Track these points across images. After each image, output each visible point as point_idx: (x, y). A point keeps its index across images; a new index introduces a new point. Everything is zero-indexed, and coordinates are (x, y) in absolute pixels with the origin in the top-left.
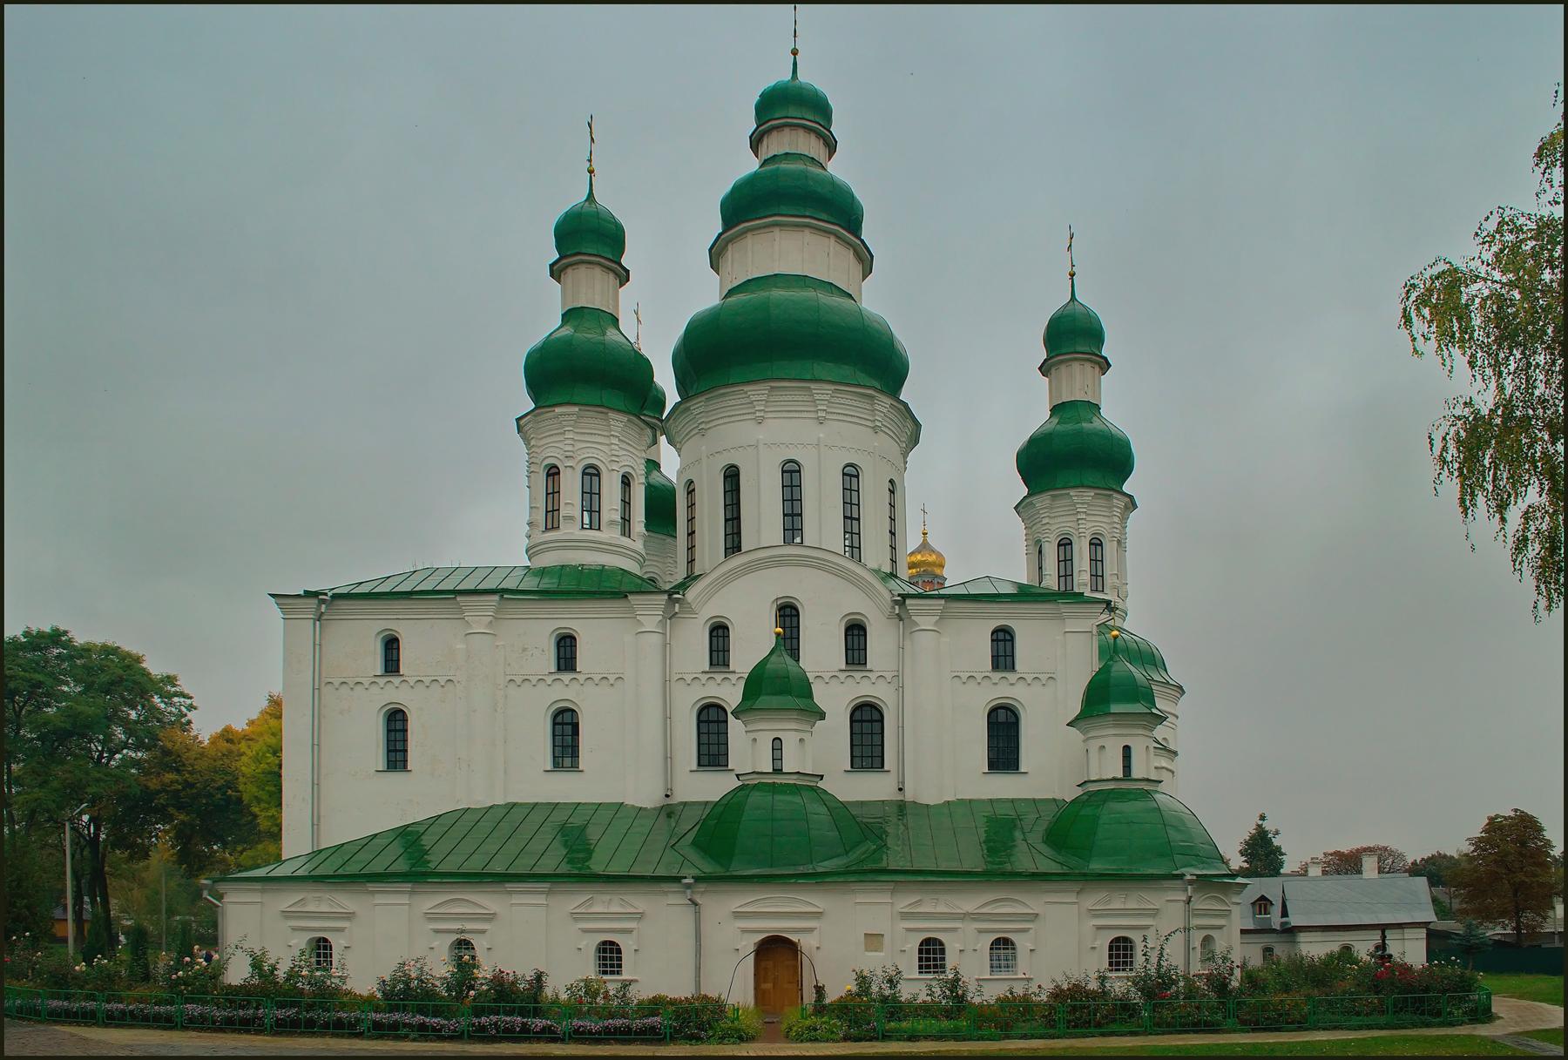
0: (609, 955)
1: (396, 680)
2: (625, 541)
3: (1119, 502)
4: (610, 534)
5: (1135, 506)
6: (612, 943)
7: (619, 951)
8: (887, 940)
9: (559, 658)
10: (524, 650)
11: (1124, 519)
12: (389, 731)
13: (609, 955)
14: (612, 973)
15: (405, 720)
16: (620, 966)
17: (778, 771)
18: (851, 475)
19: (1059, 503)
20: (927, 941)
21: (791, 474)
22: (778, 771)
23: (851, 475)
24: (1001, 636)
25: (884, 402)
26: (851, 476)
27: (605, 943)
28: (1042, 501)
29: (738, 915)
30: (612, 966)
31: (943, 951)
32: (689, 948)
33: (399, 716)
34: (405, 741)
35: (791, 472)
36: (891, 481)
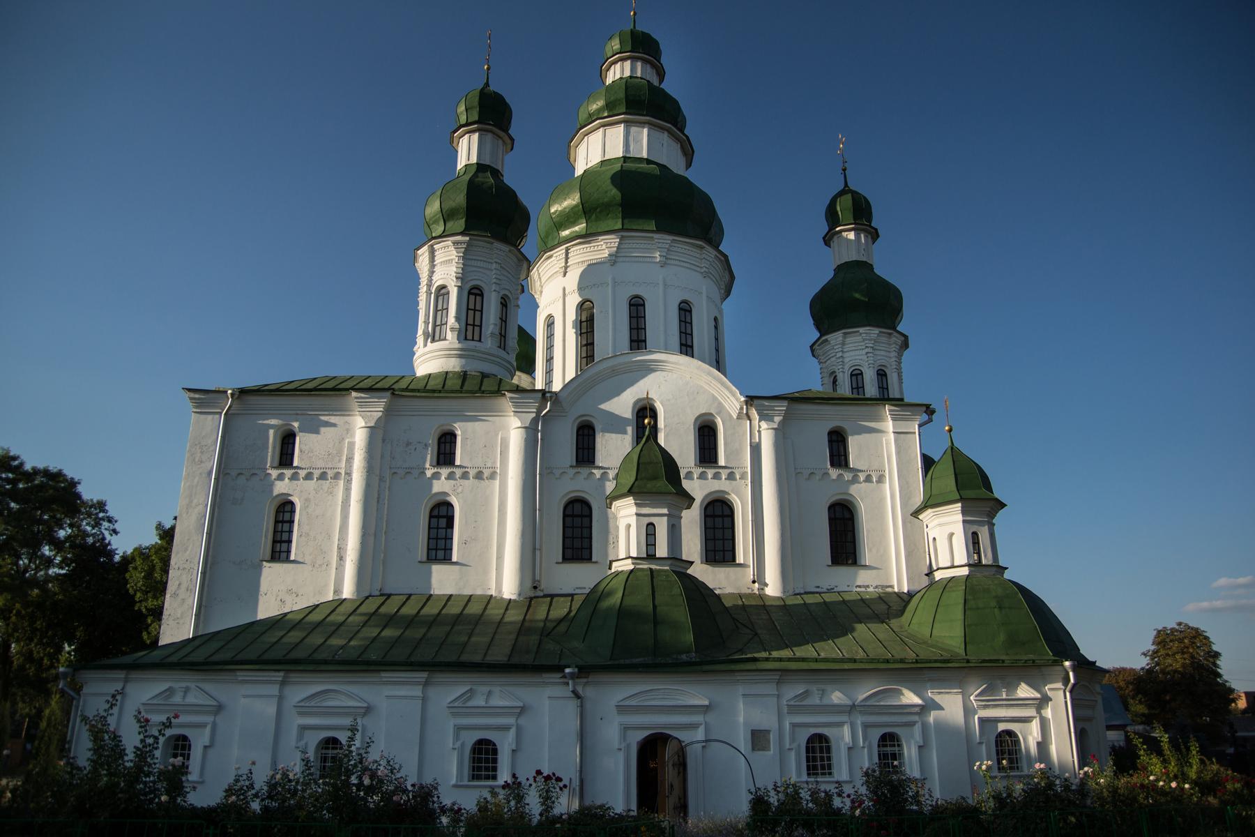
0: (483, 757)
1: (288, 473)
2: (502, 353)
3: (900, 340)
4: (489, 343)
5: (905, 345)
6: (488, 742)
7: (495, 751)
8: (773, 737)
9: (439, 454)
10: (408, 444)
11: (900, 356)
12: (277, 522)
13: (483, 757)
14: (487, 778)
15: (293, 511)
16: (495, 769)
17: (651, 557)
18: (685, 310)
19: (848, 340)
20: (811, 739)
21: (637, 307)
22: (651, 557)
23: (685, 310)
24: (834, 438)
25: (710, 252)
26: (686, 310)
27: (480, 742)
28: (835, 338)
29: (622, 709)
30: (487, 769)
31: (829, 749)
32: (569, 740)
33: (288, 508)
34: (291, 532)
35: (637, 305)
36: (716, 319)
